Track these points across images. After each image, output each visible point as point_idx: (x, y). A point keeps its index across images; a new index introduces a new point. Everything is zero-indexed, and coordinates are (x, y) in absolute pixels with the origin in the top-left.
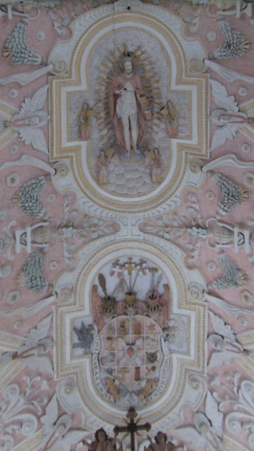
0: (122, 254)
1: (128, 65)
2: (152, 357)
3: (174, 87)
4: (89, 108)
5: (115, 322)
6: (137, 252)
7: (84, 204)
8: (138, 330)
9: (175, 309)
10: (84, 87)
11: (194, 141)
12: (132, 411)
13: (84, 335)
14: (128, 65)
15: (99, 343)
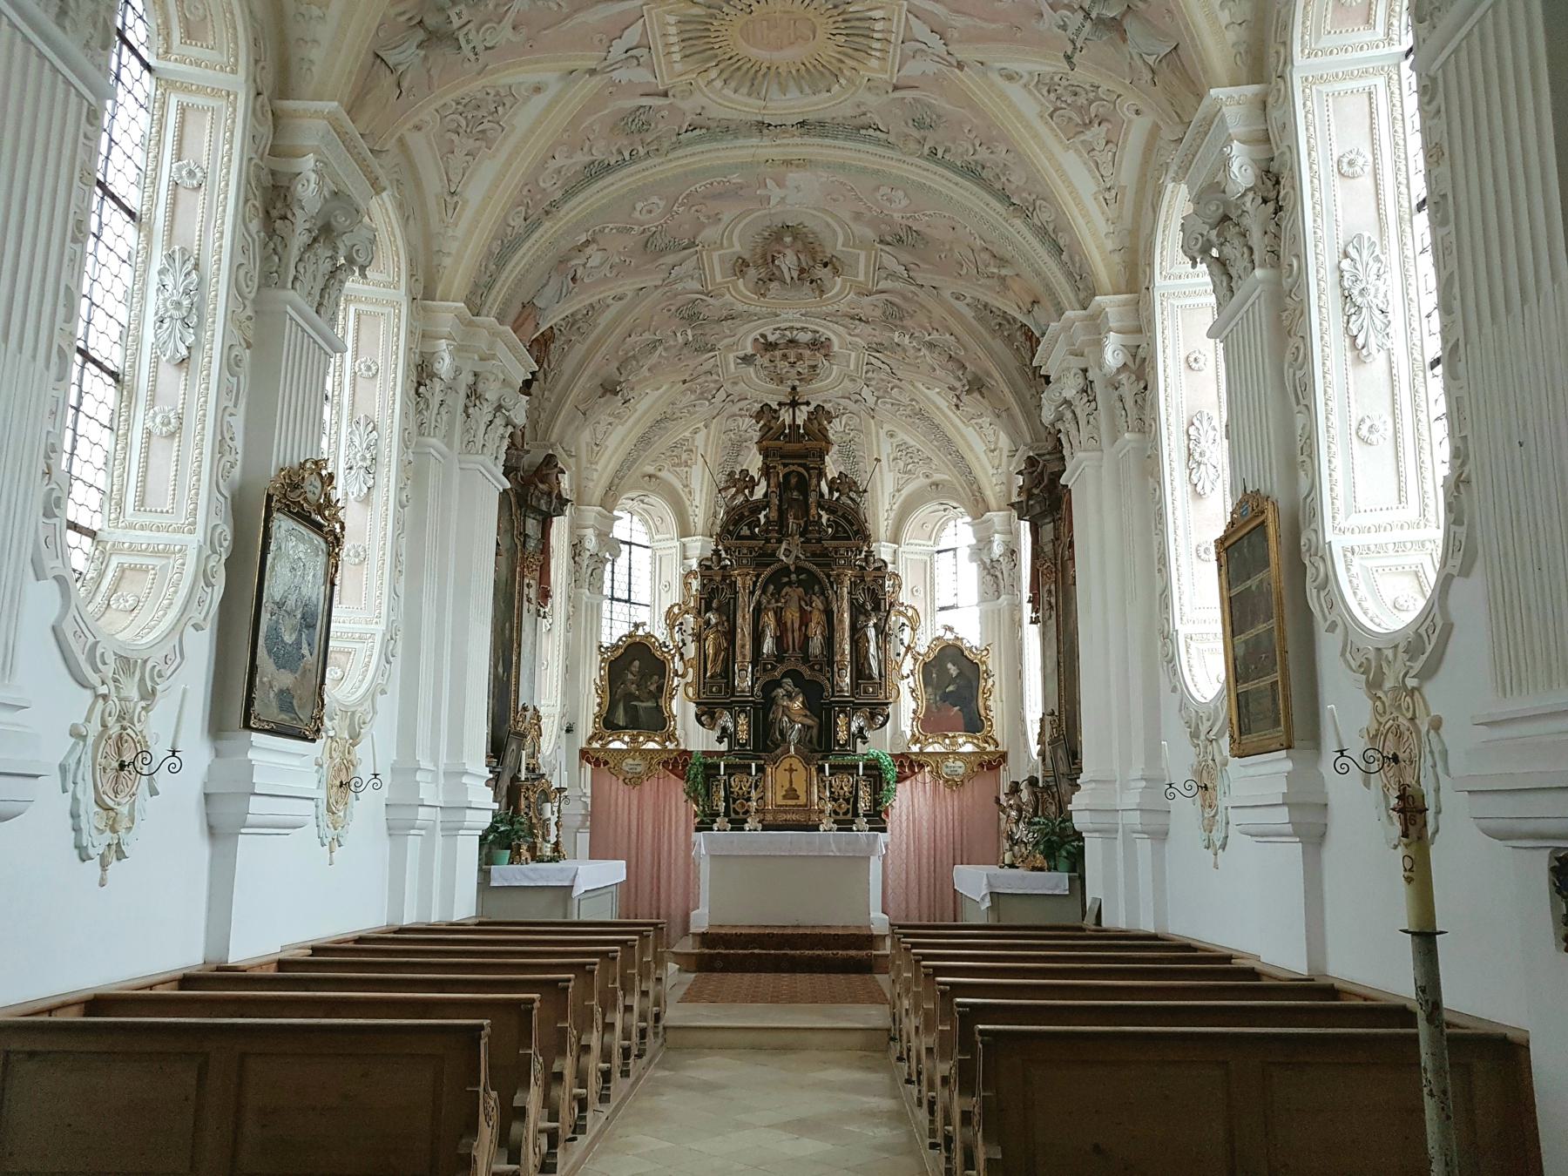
0: (783, 325)
1: (788, 240)
2: (814, 367)
3: (839, 247)
4: (745, 263)
5: (778, 353)
6: (799, 325)
7: (740, 307)
8: (800, 357)
9: (836, 348)
10: (737, 248)
11: (861, 278)
12: (794, 388)
13: (747, 360)
14: (788, 240)
15: (758, 360)
